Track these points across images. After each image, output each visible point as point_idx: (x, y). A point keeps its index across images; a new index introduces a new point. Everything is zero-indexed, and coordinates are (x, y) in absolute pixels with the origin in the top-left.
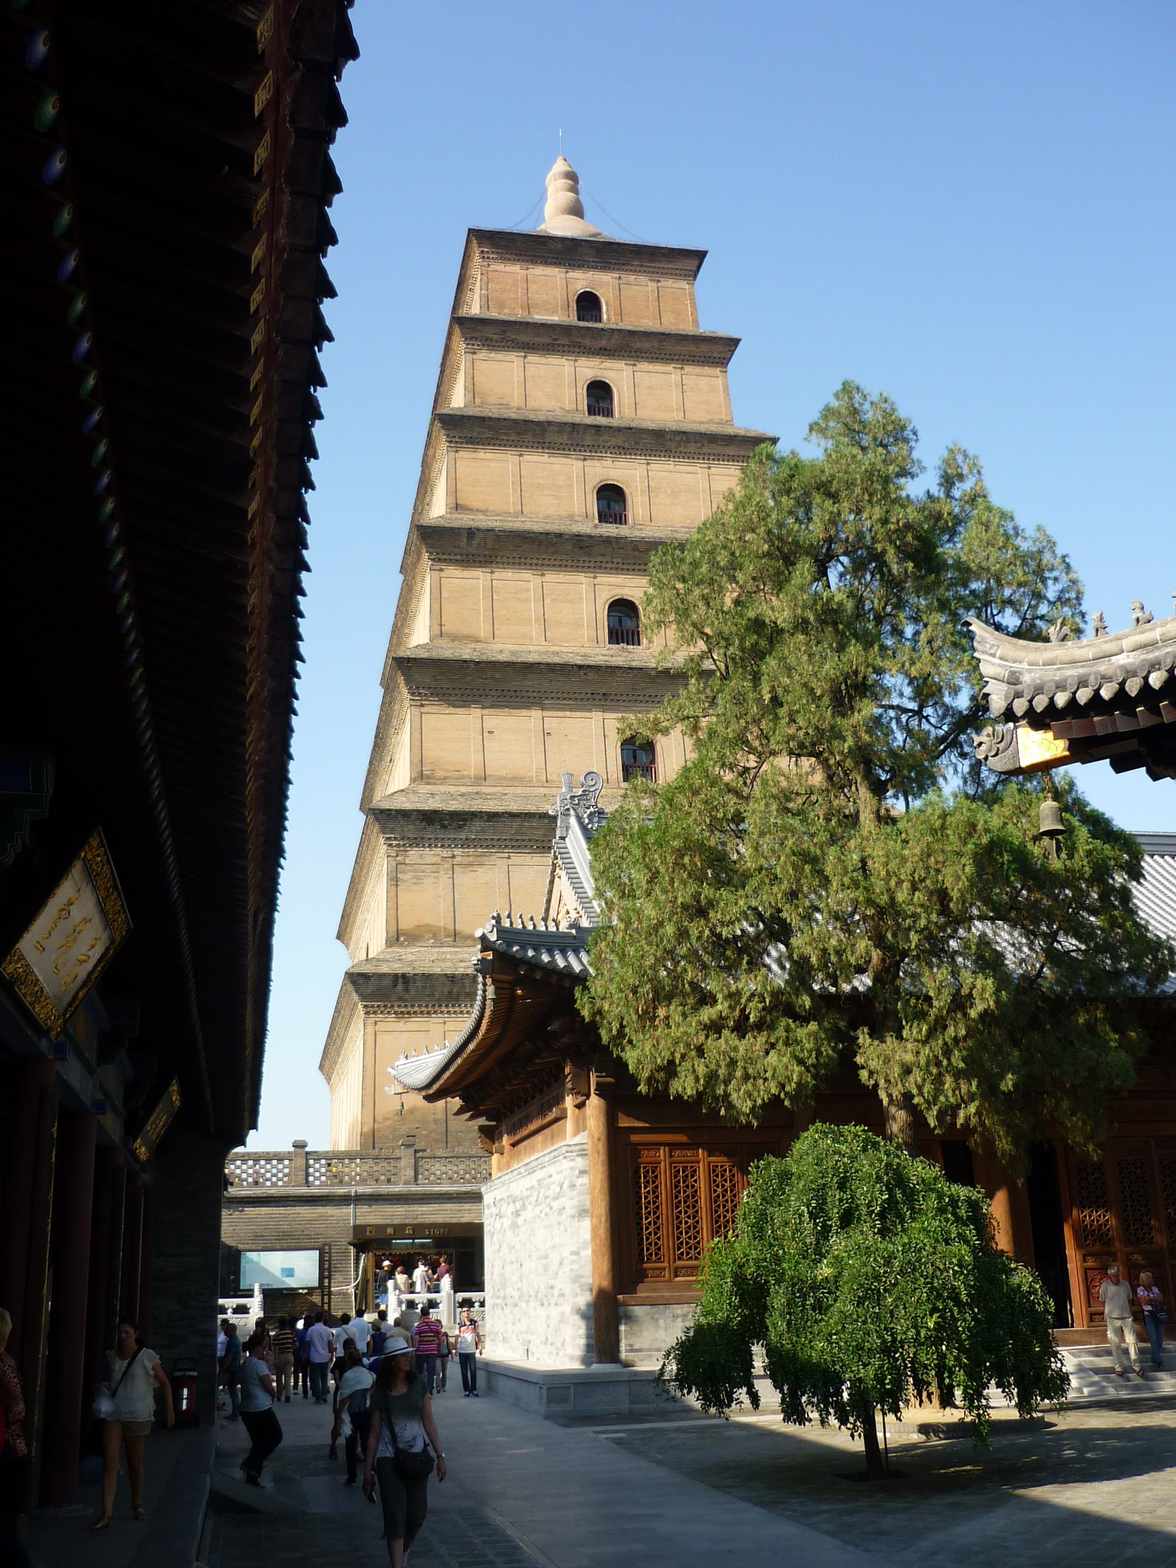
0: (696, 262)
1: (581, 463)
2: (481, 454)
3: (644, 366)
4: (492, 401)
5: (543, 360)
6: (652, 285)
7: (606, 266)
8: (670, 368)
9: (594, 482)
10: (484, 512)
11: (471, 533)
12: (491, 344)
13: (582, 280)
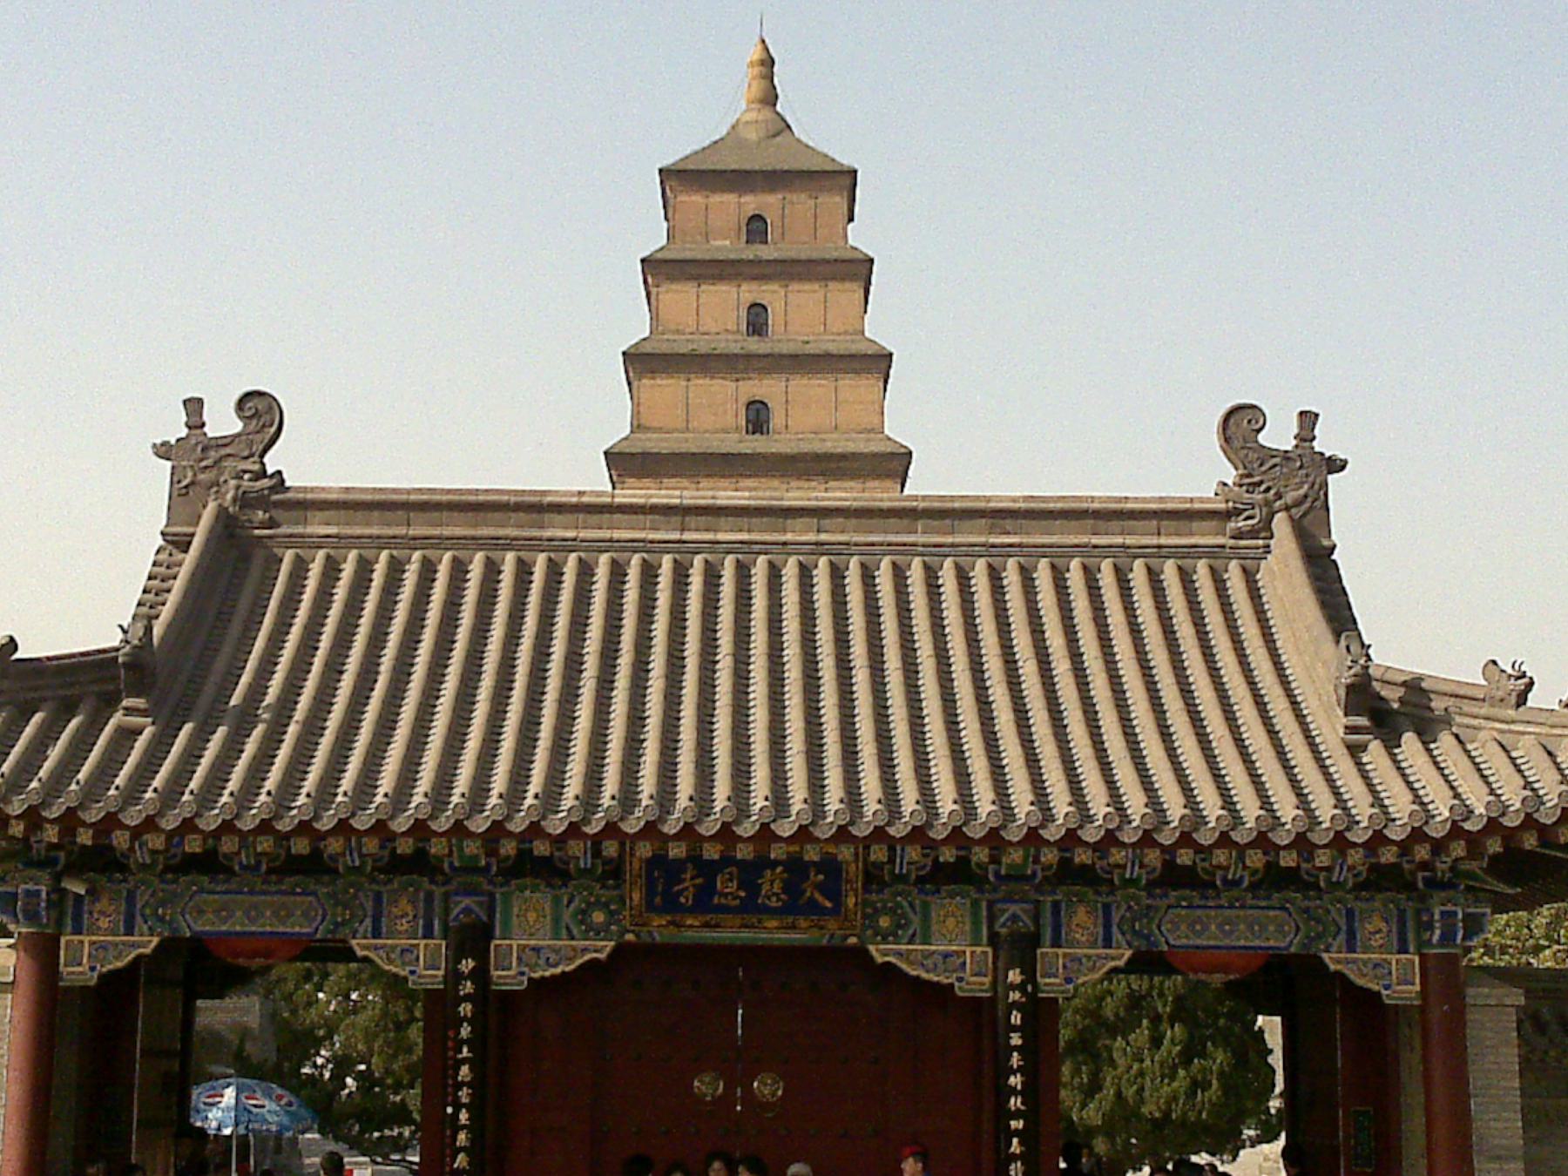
0: (848, 181)
1: (734, 385)
2: (659, 382)
3: (794, 286)
4: (673, 327)
5: (712, 288)
6: (812, 202)
7: (772, 190)
8: (816, 286)
9: (743, 400)
10: (659, 430)
11: (645, 455)
12: (672, 279)
13: (751, 203)
